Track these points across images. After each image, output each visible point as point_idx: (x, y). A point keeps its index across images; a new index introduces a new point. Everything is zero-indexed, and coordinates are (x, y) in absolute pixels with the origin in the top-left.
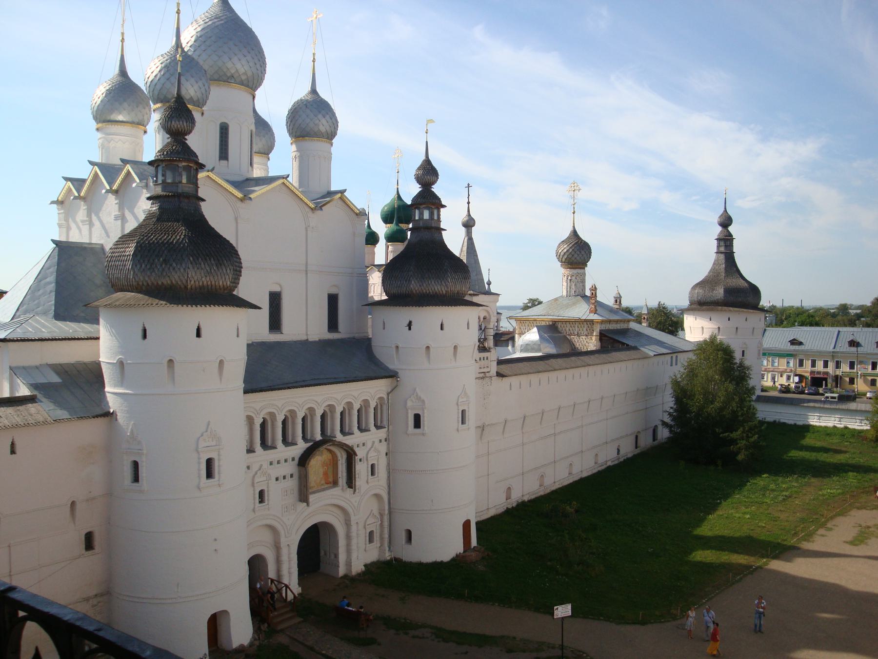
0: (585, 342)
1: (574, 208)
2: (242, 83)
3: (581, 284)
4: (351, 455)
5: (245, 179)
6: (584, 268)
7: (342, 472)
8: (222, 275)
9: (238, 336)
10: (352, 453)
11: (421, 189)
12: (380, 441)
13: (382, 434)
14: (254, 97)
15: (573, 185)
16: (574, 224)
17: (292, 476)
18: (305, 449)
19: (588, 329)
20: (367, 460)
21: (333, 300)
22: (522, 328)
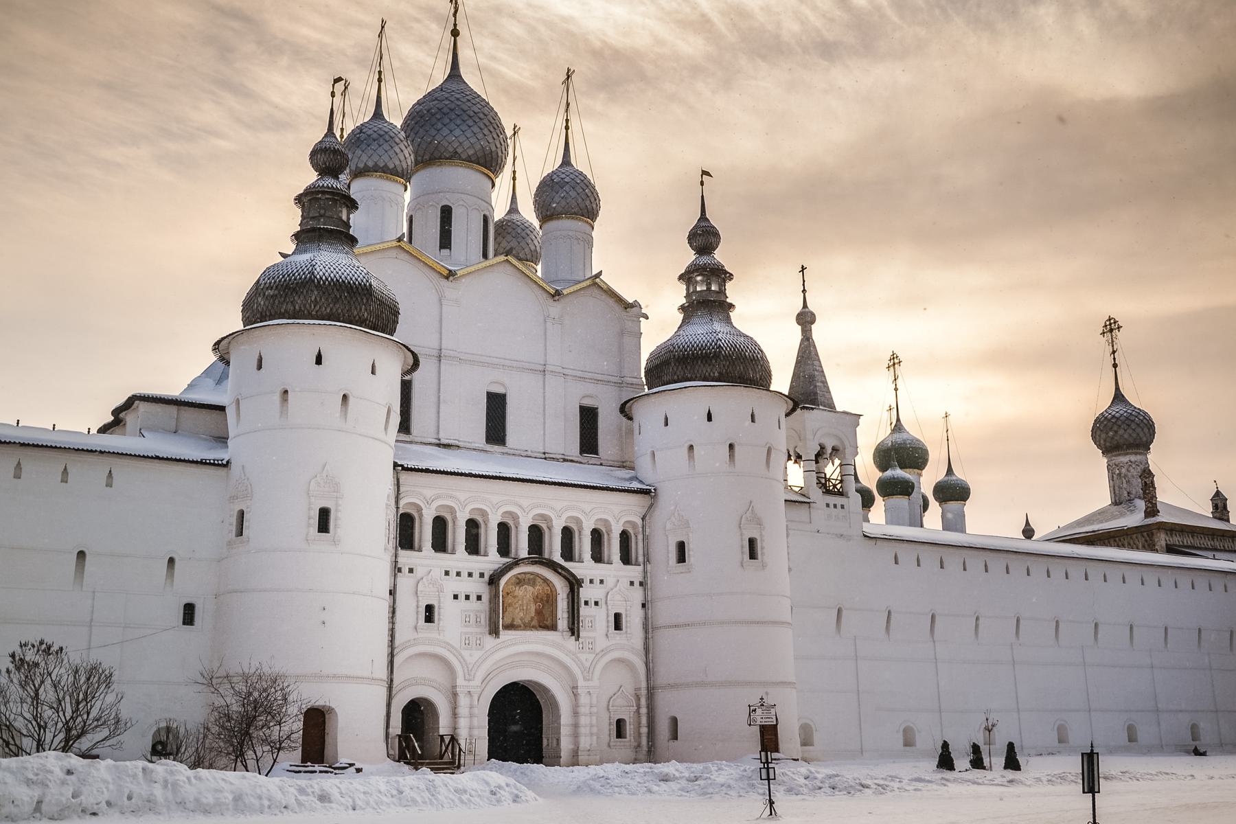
1: (1114, 359)
2: (469, 160)
4: (574, 584)
8: (357, 304)
10: (574, 581)
12: (632, 583)
13: (634, 572)
15: (1108, 323)
17: (479, 598)
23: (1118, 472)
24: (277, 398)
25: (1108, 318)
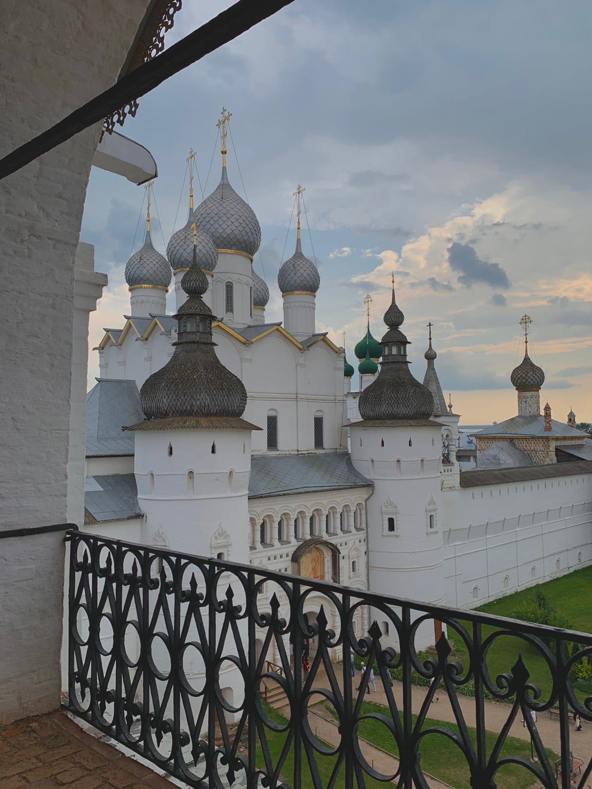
0: (542, 457)
1: (526, 338)
3: (536, 406)
4: (335, 552)
5: (247, 326)
6: (538, 391)
7: (328, 568)
9: (244, 452)
10: (336, 550)
11: (389, 330)
12: (360, 541)
13: (362, 535)
14: (252, 260)
15: (524, 318)
16: (526, 351)
18: (297, 547)
19: (544, 445)
20: (349, 557)
21: (318, 423)
22: (482, 444)
23: (524, 400)
24: (186, 476)
25: (524, 315)
